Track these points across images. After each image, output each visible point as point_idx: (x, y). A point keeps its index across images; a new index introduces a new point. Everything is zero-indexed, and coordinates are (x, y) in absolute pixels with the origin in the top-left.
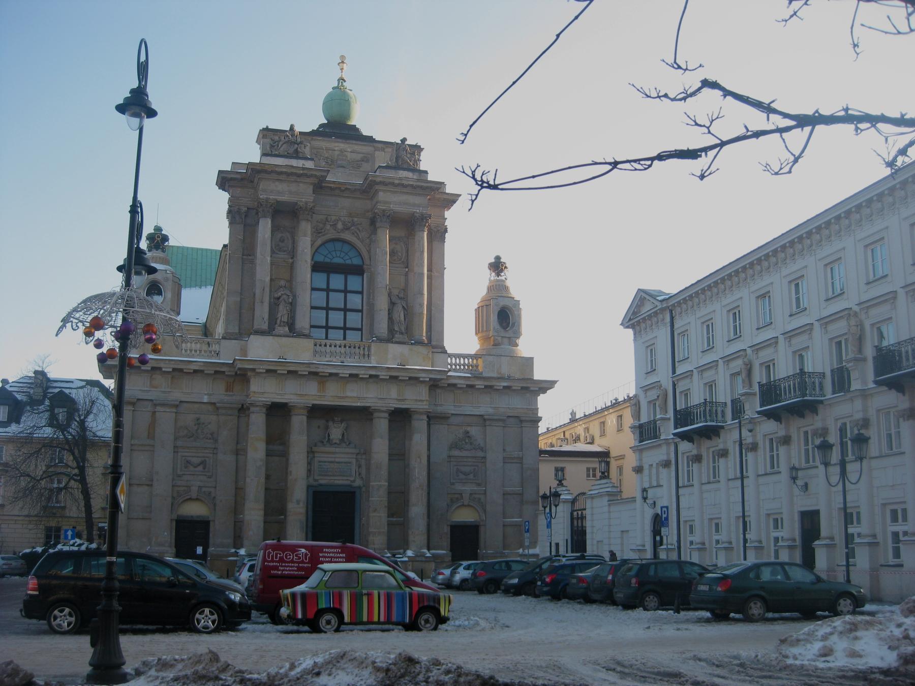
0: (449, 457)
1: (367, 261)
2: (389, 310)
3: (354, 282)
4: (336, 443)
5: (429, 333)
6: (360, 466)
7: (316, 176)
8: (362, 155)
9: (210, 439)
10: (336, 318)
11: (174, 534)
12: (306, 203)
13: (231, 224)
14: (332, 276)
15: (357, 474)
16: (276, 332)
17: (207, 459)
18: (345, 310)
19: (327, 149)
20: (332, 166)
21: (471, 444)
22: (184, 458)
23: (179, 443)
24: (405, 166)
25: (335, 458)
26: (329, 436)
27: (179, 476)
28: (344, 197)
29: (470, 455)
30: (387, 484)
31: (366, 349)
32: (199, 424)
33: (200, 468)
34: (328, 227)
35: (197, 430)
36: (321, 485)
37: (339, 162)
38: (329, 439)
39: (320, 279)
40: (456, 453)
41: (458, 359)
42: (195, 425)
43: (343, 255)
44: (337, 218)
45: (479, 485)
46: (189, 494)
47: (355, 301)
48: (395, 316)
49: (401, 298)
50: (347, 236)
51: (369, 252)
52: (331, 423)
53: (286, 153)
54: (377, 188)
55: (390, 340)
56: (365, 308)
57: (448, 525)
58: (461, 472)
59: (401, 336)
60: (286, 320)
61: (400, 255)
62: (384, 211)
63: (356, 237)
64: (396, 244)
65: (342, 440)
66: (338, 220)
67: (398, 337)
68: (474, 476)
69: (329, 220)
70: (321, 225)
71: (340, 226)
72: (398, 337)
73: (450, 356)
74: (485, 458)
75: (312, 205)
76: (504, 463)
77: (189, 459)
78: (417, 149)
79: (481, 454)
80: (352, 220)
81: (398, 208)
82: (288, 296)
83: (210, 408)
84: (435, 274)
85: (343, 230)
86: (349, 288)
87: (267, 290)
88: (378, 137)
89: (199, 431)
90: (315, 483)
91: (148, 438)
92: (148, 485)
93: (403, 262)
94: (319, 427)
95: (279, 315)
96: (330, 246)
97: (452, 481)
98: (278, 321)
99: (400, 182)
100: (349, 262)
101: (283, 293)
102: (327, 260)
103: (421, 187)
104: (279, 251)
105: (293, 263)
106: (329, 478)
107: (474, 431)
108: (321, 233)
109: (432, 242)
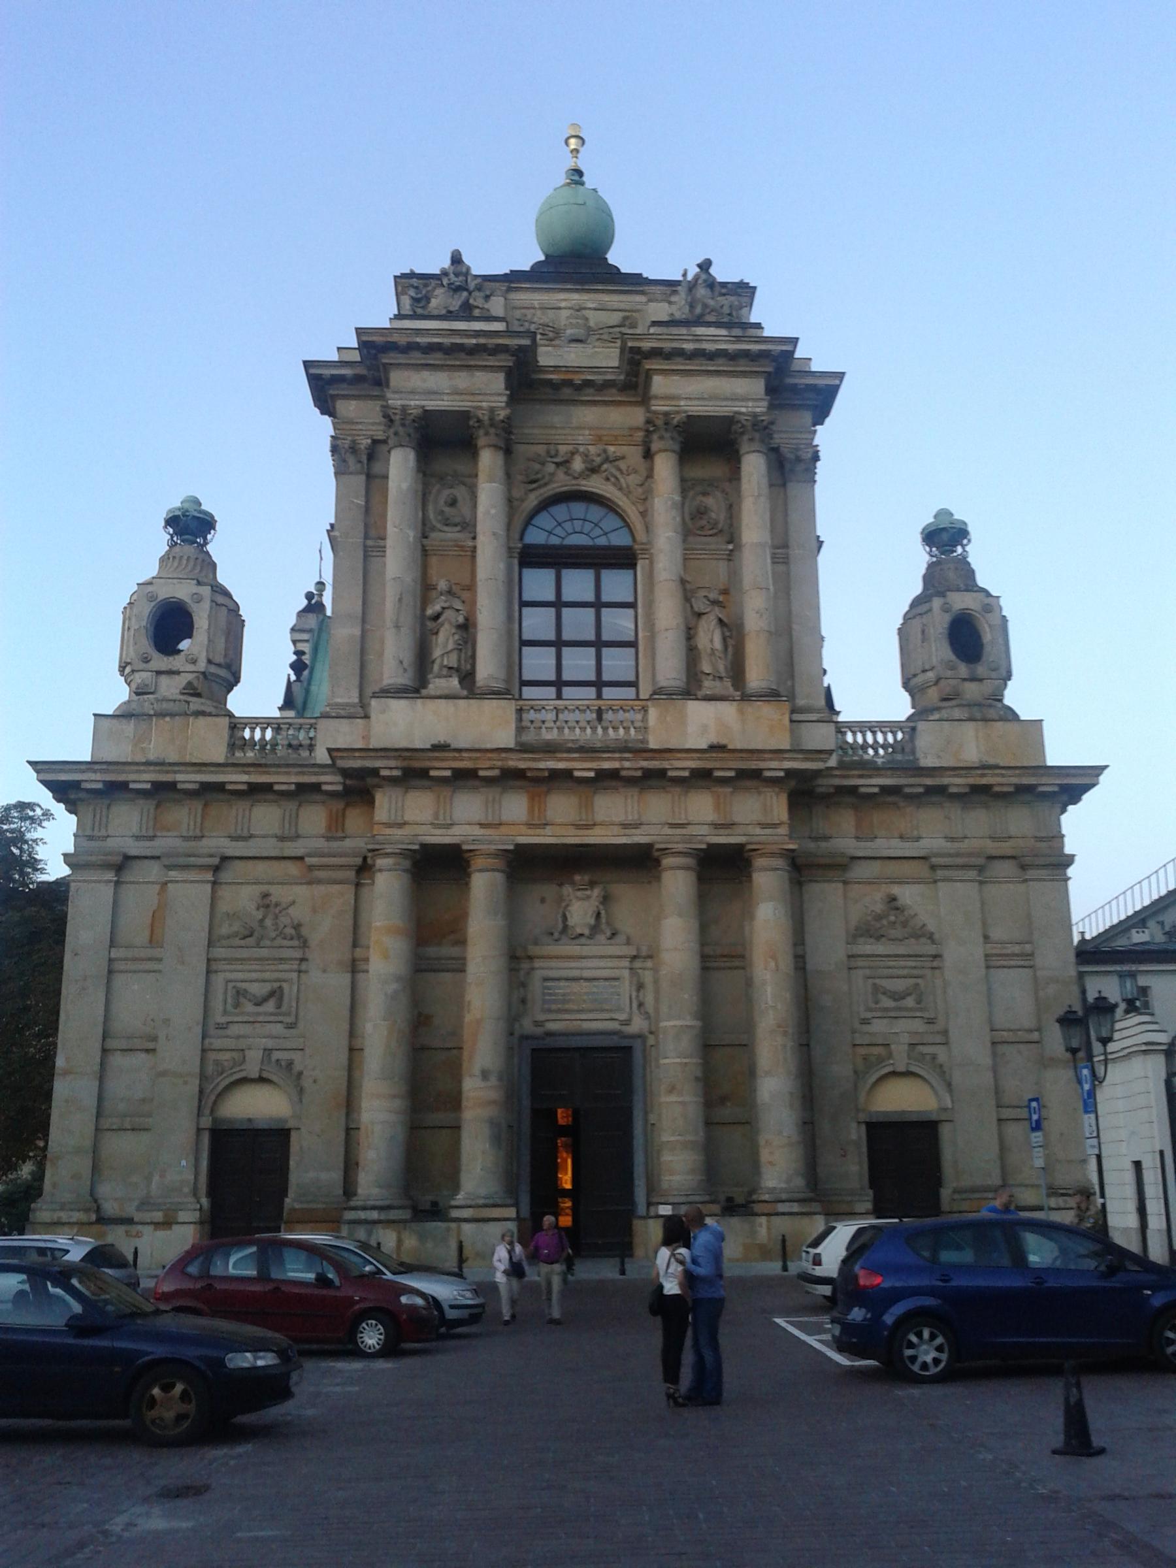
1: (641, 536)
3: (616, 584)
4: (582, 935)
5: (789, 683)
6: (640, 987)
7: (504, 349)
8: (621, 314)
9: (292, 939)
10: (579, 663)
12: (492, 410)
13: (337, 474)
15: (635, 1005)
17: (285, 985)
19: (544, 308)
20: (557, 342)
21: (905, 924)
22: (231, 985)
24: (711, 318)
25: (582, 969)
26: (565, 918)
27: (220, 1027)
32: (268, 906)
33: (270, 1006)
34: (551, 468)
35: (262, 921)
36: (550, 1034)
37: (569, 332)
39: (539, 583)
40: (868, 947)
42: (258, 909)
43: (588, 527)
46: (243, 1067)
47: (619, 623)
49: (715, 603)
50: (595, 485)
51: (644, 514)
52: (567, 890)
54: (648, 367)
56: (640, 635)
57: (859, 1123)
58: (884, 993)
59: (718, 683)
62: (666, 414)
63: (614, 485)
64: (705, 494)
65: (595, 929)
68: (919, 1002)
69: (553, 453)
70: (537, 466)
71: (578, 465)
72: (709, 686)
76: (988, 967)
77: (239, 985)
78: (744, 291)
79: (931, 949)
80: (605, 451)
82: (458, 610)
83: (293, 869)
86: (605, 598)
88: (651, 272)
89: (268, 922)
90: (539, 1031)
91: (151, 941)
92: (147, 1051)
93: (721, 531)
95: (437, 653)
96: (560, 511)
98: (436, 667)
99: (697, 346)
100: (602, 541)
101: (446, 605)
102: (555, 541)
104: (447, 525)
106: (567, 1016)
107: (907, 895)
109: (784, 485)
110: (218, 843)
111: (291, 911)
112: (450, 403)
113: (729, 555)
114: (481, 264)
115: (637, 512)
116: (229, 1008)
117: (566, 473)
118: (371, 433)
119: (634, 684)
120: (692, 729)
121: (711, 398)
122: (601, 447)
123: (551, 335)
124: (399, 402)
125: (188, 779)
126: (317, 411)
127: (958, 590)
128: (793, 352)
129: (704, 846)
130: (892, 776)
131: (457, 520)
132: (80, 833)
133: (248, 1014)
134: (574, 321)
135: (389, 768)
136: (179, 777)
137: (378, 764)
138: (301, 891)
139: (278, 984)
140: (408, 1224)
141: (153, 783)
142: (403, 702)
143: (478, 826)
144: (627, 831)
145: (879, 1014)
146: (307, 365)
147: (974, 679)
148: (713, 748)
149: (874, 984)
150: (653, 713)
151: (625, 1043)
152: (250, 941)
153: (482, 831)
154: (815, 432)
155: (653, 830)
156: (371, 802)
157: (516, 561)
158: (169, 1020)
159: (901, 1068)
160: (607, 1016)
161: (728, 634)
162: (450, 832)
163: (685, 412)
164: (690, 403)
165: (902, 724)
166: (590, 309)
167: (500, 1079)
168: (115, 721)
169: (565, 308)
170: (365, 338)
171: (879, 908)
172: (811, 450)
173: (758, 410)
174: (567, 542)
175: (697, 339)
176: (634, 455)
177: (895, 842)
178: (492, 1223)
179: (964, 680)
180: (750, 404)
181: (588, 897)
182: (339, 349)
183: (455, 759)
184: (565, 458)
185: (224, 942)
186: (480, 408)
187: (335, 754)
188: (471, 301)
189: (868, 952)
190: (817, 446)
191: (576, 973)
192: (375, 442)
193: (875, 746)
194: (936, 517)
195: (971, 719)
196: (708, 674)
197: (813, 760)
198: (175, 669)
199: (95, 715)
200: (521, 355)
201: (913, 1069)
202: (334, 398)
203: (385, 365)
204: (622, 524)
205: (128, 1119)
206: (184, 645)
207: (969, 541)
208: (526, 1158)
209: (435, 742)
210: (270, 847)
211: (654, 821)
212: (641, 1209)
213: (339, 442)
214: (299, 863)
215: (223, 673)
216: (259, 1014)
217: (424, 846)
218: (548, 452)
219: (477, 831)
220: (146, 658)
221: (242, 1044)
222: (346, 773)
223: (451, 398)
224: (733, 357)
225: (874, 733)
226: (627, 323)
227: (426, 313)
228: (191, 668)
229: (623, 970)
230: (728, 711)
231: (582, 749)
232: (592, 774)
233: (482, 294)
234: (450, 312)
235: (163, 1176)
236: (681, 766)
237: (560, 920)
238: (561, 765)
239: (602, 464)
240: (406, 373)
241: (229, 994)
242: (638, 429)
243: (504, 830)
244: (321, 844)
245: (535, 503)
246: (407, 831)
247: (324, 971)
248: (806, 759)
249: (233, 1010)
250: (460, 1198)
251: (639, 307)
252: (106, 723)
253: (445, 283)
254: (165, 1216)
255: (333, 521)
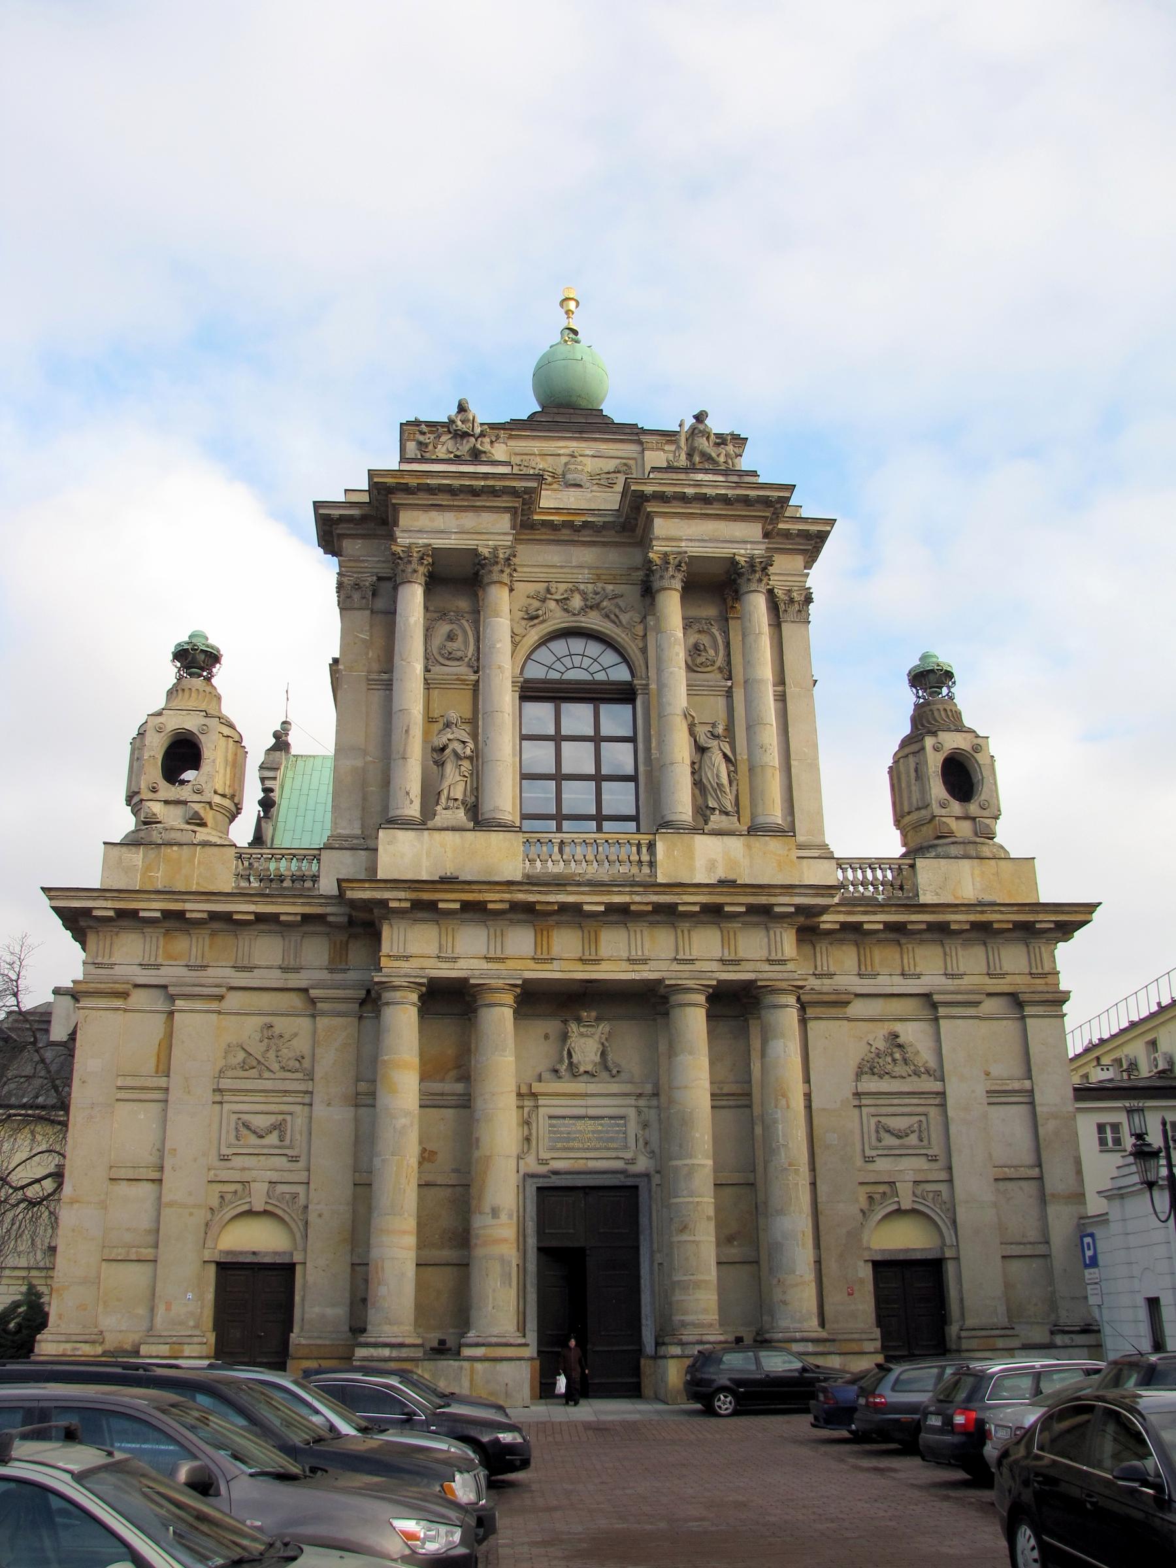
0: (857, 1095)
2: (693, 763)
3: (616, 719)
4: (586, 1072)
6: (645, 1125)
7: (513, 492)
8: (618, 461)
9: (297, 1071)
10: (579, 797)
11: (210, 1296)
12: (496, 548)
14: (567, 707)
15: (641, 1142)
16: (438, 821)
18: (598, 778)
20: (555, 486)
21: (906, 1061)
22: (235, 1117)
23: (225, 1084)
26: (570, 1055)
28: (584, 543)
29: (906, 1089)
30: (710, 1162)
31: (644, 850)
33: (273, 1139)
36: (556, 1173)
37: (569, 476)
38: (571, 1064)
39: (541, 715)
40: (871, 1084)
41: (859, 871)
43: (587, 662)
44: (570, 585)
45: (933, 1159)
48: (709, 776)
49: (715, 737)
50: (593, 621)
52: (573, 1027)
53: (452, 456)
55: (698, 829)
56: (641, 768)
58: (888, 1131)
59: (724, 817)
60: (459, 796)
61: (712, 652)
62: (666, 554)
66: (571, 590)
67: (717, 821)
69: (553, 590)
70: (536, 604)
72: (717, 821)
73: (841, 864)
74: (943, 1094)
75: (508, 552)
80: (604, 589)
81: (695, 550)
82: (464, 742)
83: (295, 1000)
84: (791, 690)
85: (584, 610)
86: (604, 732)
87: (417, 732)
90: (543, 1169)
91: (157, 1072)
93: (719, 668)
94: (546, 1037)
95: (445, 785)
97: (868, 1153)
99: (697, 490)
100: (601, 676)
103: (746, 501)
104: (449, 659)
105: (478, 681)
106: (572, 1155)
108: (537, 617)
110: (221, 973)
111: (294, 1042)
112: (456, 542)
113: (727, 692)
114: (483, 413)
115: (637, 651)
116: (234, 1141)
117: (566, 610)
118: (375, 570)
119: (635, 818)
120: (700, 863)
121: (710, 540)
122: (600, 585)
123: (550, 479)
124: (408, 541)
125: (196, 909)
126: (321, 551)
127: (949, 730)
128: (789, 499)
129: (714, 983)
130: (896, 913)
131: (459, 654)
132: (90, 961)
133: (254, 1147)
134: (572, 467)
135: (397, 899)
136: (188, 906)
137: (386, 895)
138: (304, 1023)
139: (280, 1117)
140: (420, 1363)
141: (163, 911)
142: (411, 834)
143: (485, 960)
144: (636, 967)
145: (885, 1152)
146: (317, 505)
147: (967, 817)
148: (722, 883)
149: (879, 1122)
150: (660, 847)
151: (630, 1182)
152: (253, 1073)
153: (491, 966)
154: (808, 575)
155: (664, 966)
156: (376, 937)
157: (517, 695)
158: (175, 1150)
159: (906, 1205)
160: (614, 1155)
161: (732, 769)
162: (457, 965)
163: (686, 552)
164: (690, 544)
165: (901, 861)
166: (587, 456)
167: (510, 1217)
168: (124, 849)
169: (563, 455)
170: (376, 480)
171: (881, 1045)
172: (804, 593)
173: (756, 552)
174: (565, 677)
175: (698, 484)
176: (631, 593)
177: (898, 980)
178: (505, 1364)
179: (957, 818)
180: (749, 546)
181: (592, 1036)
182: (346, 490)
183: (463, 891)
184: (565, 596)
185: (230, 1073)
186: (487, 546)
187: (344, 885)
188: (478, 446)
189: (874, 1090)
190: (810, 588)
191: (582, 1111)
192: (380, 579)
193: (875, 883)
194: (920, 659)
195: (966, 857)
196: (714, 809)
197: (823, 895)
198: (182, 799)
199: (105, 843)
200: (526, 496)
201: (917, 1206)
202: (341, 536)
203: (394, 505)
204: (619, 660)
205: (134, 1249)
206: (189, 775)
207: (954, 683)
208: (532, 1297)
209: (443, 874)
210: (274, 978)
211: (663, 956)
212: (649, 1347)
213: (345, 580)
214: (302, 995)
215: (227, 803)
216: (264, 1147)
217: (432, 981)
218: (548, 591)
219: (484, 965)
220: (154, 788)
221: (246, 1176)
222: (352, 903)
223: (458, 536)
224: (725, 500)
225: (873, 870)
226: (625, 468)
227: (434, 457)
228: (196, 798)
229: (630, 1109)
230: (735, 845)
231: (590, 883)
232: (602, 908)
233: (487, 440)
234: (456, 456)
235: (168, 1309)
236: (690, 901)
237: (566, 1056)
238: (571, 899)
239: (602, 601)
240: (415, 513)
241: (233, 1125)
242: (638, 569)
243: (510, 964)
244: (324, 975)
245: (536, 638)
246: (414, 963)
247: (329, 1105)
248: (817, 895)
249: (237, 1142)
250: (472, 1336)
251: (635, 455)
252: (116, 851)
253: (451, 430)
254: (171, 1349)
255: (337, 656)
